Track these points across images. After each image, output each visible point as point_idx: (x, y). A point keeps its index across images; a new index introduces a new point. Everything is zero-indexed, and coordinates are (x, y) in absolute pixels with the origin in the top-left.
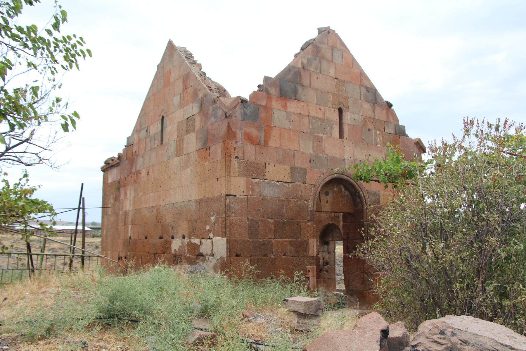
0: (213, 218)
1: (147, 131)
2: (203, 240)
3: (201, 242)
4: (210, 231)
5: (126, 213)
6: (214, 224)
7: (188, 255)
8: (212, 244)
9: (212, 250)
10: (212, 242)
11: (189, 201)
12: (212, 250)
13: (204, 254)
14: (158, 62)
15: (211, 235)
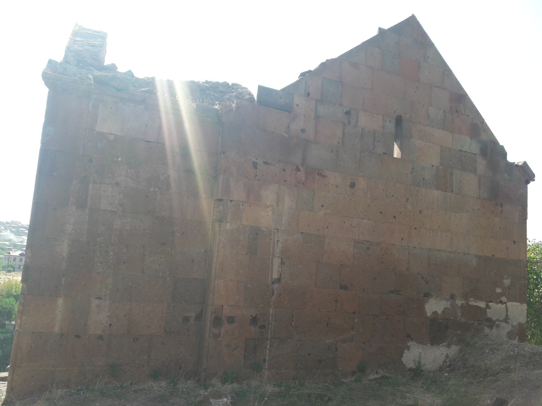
0: (507, 282)
1: (348, 113)
2: (490, 304)
3: (487, 306)
4: (502, 294)
5: (256, 232)
6: (509, 288)
7: (463, 320)
8: (507, 309)
9: (507, 315)
10: (506, 307)
11: (464, 253)
12: (507, 315)
13: (494, 319)
14: (387, 25)
15: (504, 299)
